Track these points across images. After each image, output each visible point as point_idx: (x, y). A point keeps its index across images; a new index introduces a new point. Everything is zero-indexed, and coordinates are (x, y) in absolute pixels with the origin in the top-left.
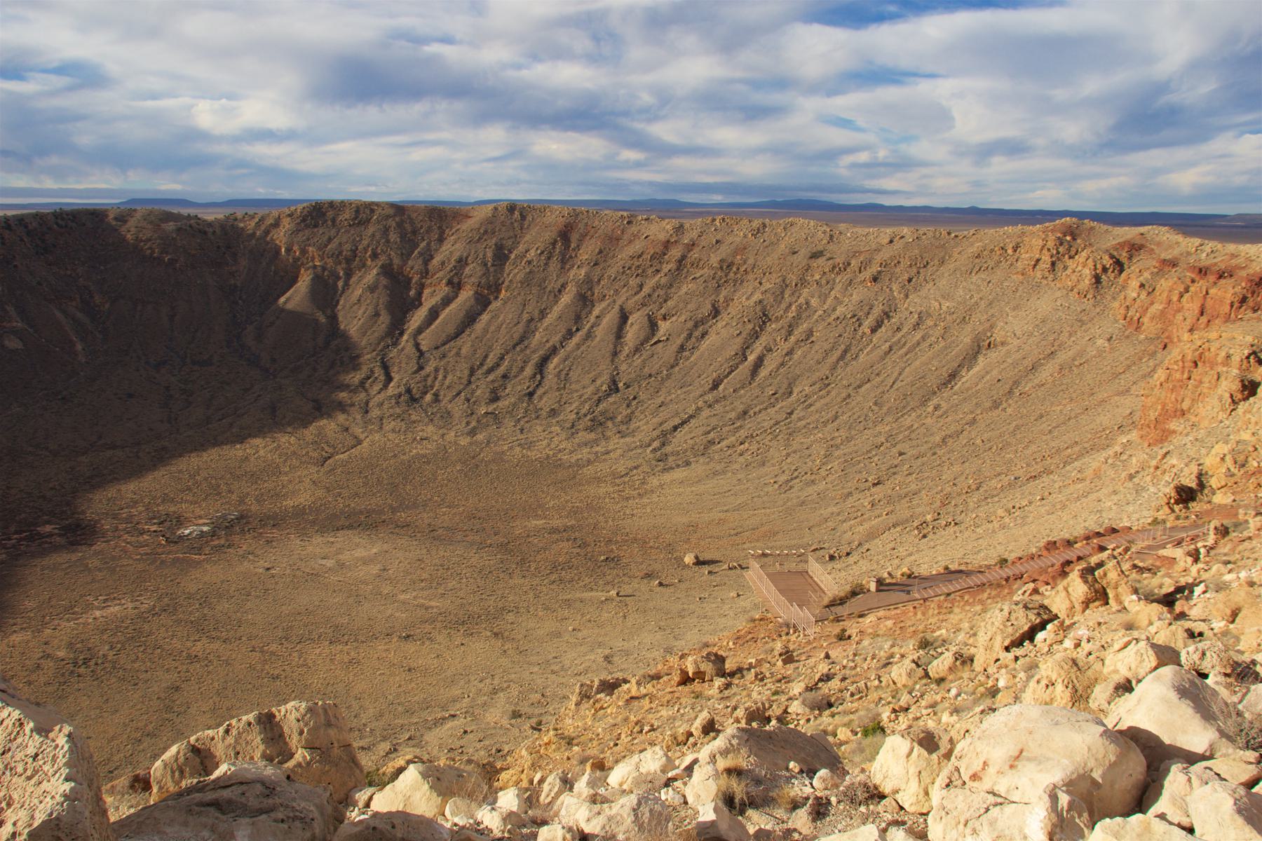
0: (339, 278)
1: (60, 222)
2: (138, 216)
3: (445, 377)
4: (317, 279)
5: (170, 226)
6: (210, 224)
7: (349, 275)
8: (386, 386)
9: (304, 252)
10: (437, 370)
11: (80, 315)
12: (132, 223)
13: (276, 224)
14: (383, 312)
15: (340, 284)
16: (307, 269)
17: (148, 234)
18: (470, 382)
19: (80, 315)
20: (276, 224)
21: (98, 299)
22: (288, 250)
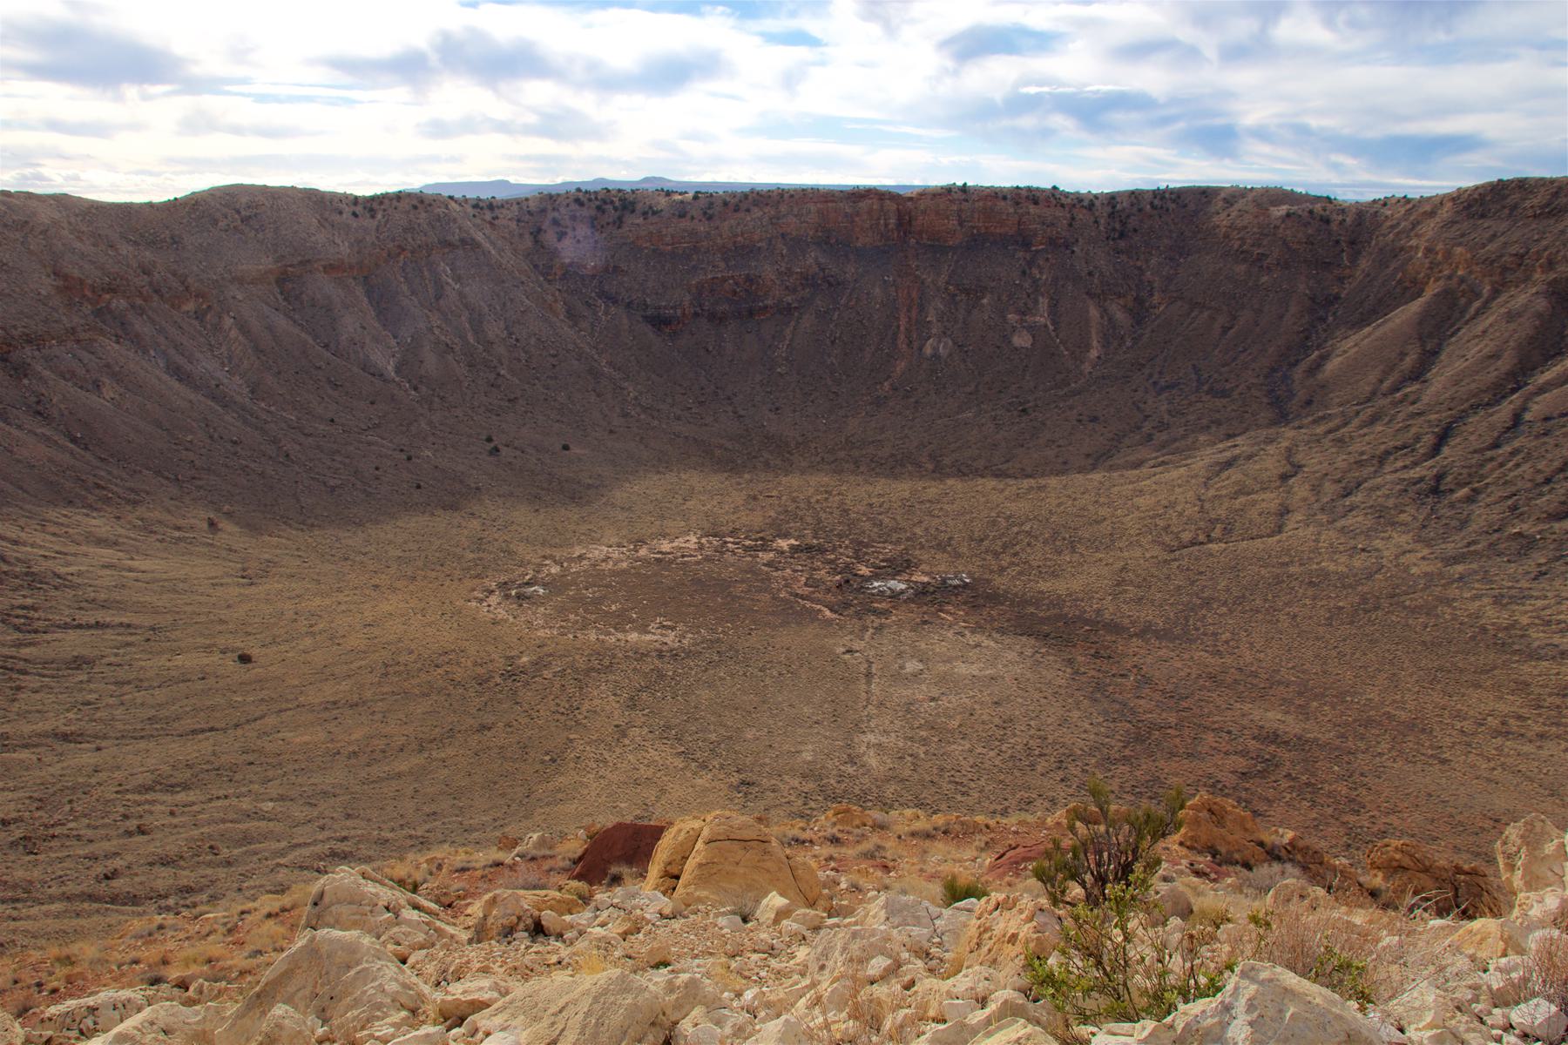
0: (1478, 295)
1: (1156, 202)
2: (1250, 197)
3: (1518, 465)
4: (1447, 296)
5: (1283, 210)
6: (1343, 211)
7: (1496, 293)
8: (1415, 464)
9: (1448, 255)
10: (1513, 453)
11: (1120, 316)
12: (1240, 204)
13: (1432, 214)
14: (1506, 354)
15: (1477, 304)
16: (1437, 280)
17: (1247, 219)
18: (1548, 481)
19: (1120, 316)
20: (1432, 214)
21: (1156, 299)
22: (1429, 250)
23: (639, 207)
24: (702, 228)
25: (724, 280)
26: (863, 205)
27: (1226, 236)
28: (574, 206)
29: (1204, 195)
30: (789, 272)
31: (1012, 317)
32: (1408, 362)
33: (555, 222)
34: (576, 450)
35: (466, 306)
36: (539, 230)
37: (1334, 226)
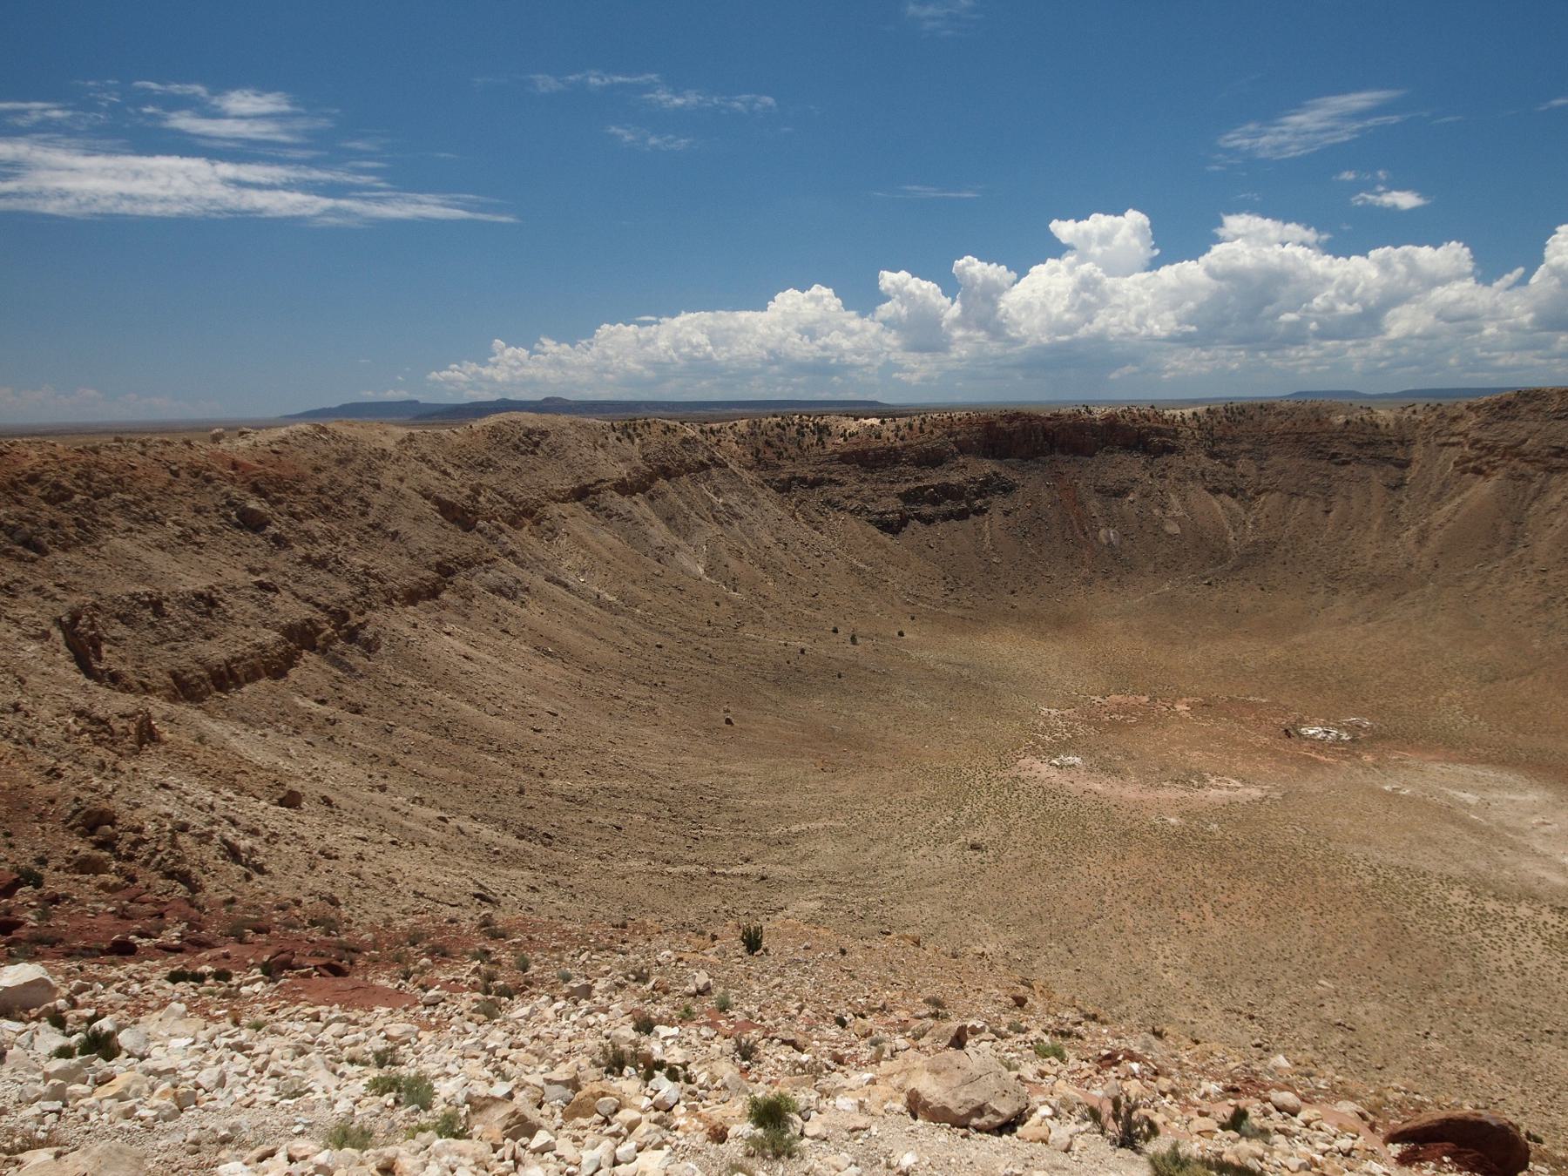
5: (1340, 419)
16: (1495, 468)
17: (1314, 428)
23: (833, 429)
24: (899, 444)
25: (927, 488)
26: (1017, 423)
27: (1298, 440)
28: (777, 430)
29: (1265, 408)
30: (975, 481)
31: (1156, 511)
32: (1504, 531)
33: (768, 444)
34: (907, 636)
35: (737, 516)
36: (758, 451)
37: (1382, 428)
